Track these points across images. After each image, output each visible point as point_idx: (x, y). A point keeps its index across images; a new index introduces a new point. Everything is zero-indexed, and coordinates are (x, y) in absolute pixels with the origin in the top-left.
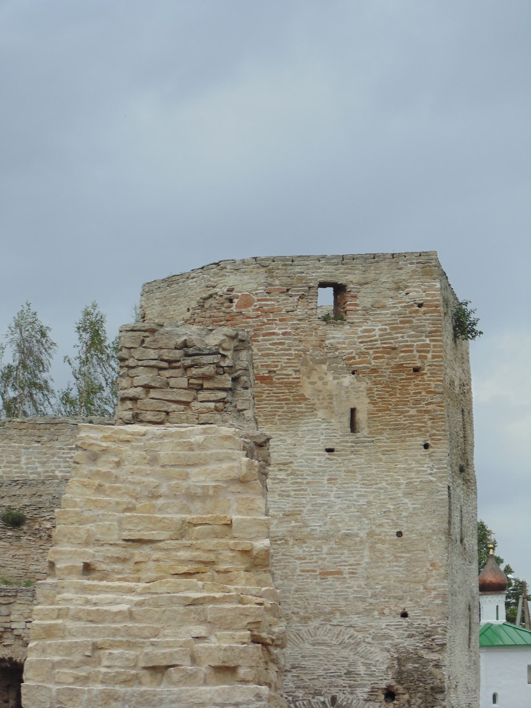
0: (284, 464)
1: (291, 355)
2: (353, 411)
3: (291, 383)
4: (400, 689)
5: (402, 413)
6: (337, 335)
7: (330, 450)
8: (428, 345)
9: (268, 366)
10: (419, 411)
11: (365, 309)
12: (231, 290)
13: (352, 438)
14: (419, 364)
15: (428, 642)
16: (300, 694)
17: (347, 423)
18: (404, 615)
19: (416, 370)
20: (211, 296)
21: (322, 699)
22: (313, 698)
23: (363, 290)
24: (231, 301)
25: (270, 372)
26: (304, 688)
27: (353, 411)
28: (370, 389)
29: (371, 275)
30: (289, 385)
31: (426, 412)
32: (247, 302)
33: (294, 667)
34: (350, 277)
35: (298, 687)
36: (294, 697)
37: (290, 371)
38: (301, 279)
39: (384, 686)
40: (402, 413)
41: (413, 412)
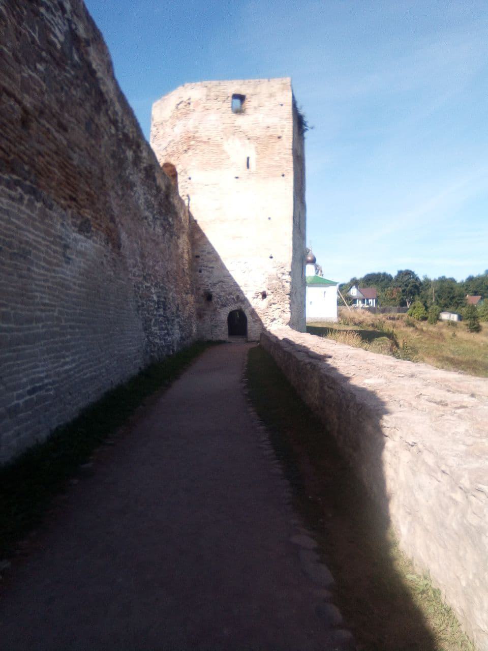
0: (215, 184)
1: (217, 131)
2: (248, 159)
3: (218, 144)
4: (268, 292)
5: (272, 159)
6: (240, 120)
7: (237, 178)
8: (285, 125)
9: (207, 136)
10: (281, 158)
11: (255, 108)
12: (189, 99)
13: (248, 171)
14: (280, 134)
15: (282, 270)
16: (223, 294)
17: (245, 164)
18: (271, 257)
19: (279, 138)
20: (181, 103)
21: (232, 296)
22: (229, 296)
23: (254, 97)
24: (189, 104)
25: (209, 139)
26: (224, 291)
27: (248, 159)
28: (256, 147)
29: (258, 90)
30: (218, 145)
31: (284, 158)
32: (197, 104)
33: (219, 282)
34: (248, 92)
35: (222, 291)
36: (219, 296)
37: (218, 138)
38: (224, 92)
39: (261, 291)
40: (272, 159)
41: (277, 158)
